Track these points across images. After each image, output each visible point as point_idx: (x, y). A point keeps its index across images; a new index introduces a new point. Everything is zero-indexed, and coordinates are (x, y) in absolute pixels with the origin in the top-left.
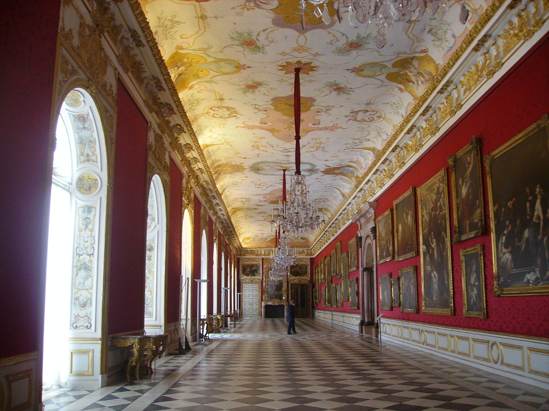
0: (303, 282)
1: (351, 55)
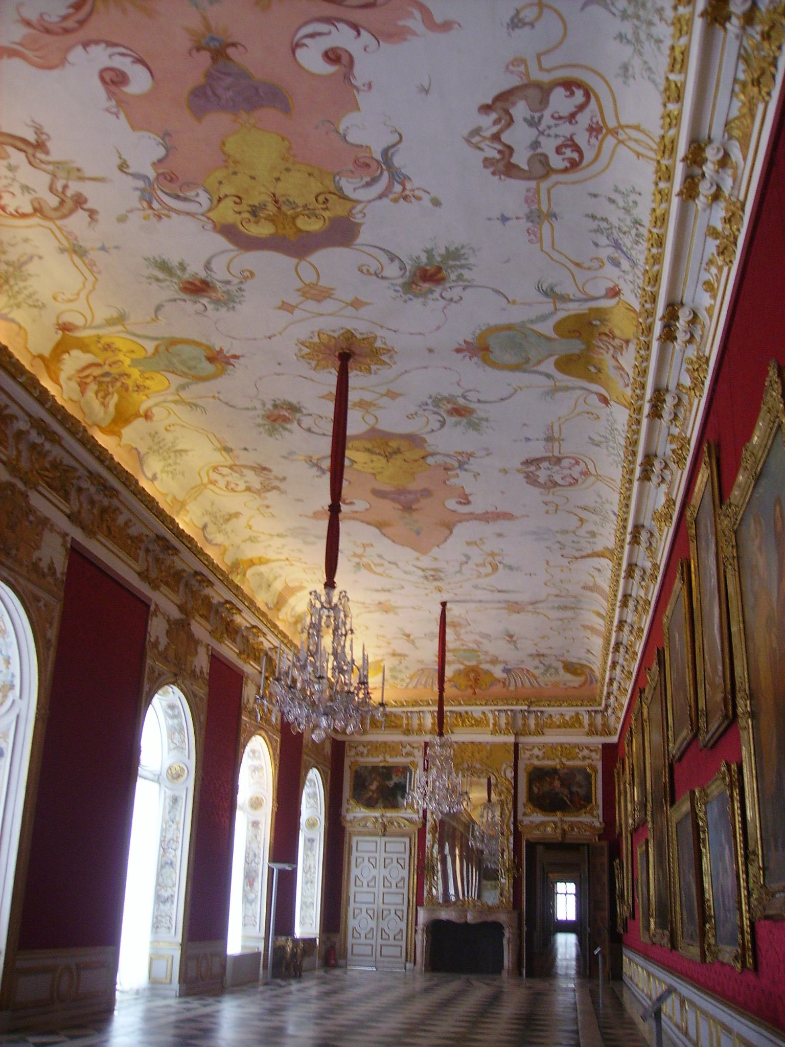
0: (574, 836)
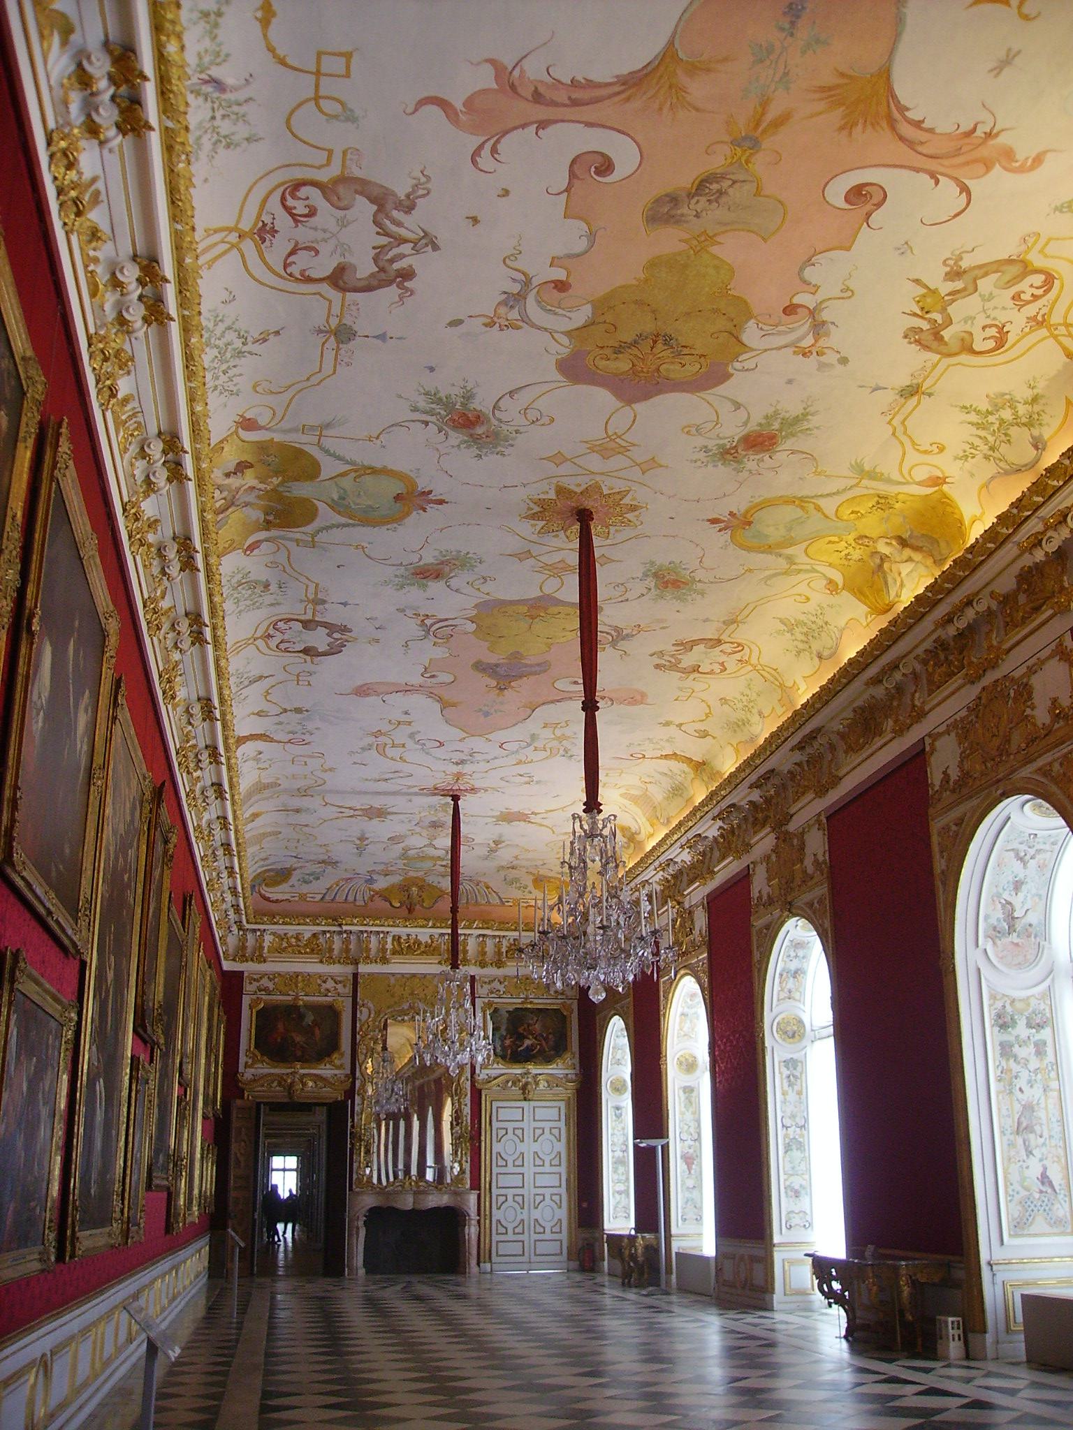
1: (437, 553)
